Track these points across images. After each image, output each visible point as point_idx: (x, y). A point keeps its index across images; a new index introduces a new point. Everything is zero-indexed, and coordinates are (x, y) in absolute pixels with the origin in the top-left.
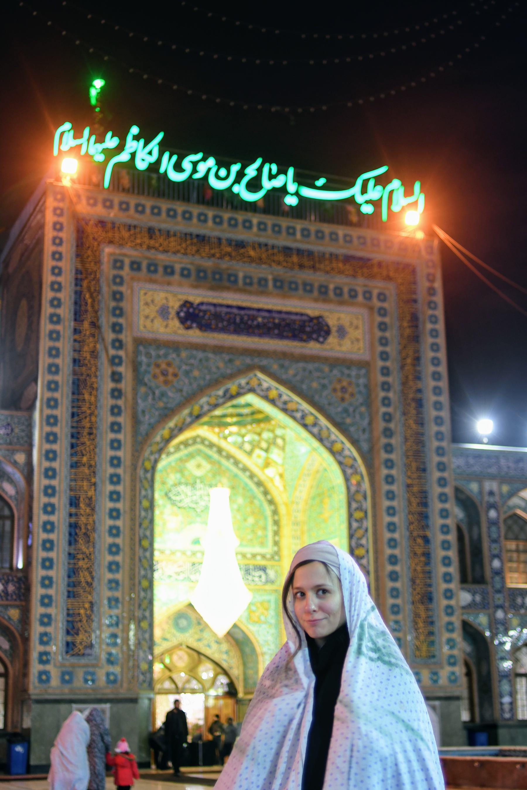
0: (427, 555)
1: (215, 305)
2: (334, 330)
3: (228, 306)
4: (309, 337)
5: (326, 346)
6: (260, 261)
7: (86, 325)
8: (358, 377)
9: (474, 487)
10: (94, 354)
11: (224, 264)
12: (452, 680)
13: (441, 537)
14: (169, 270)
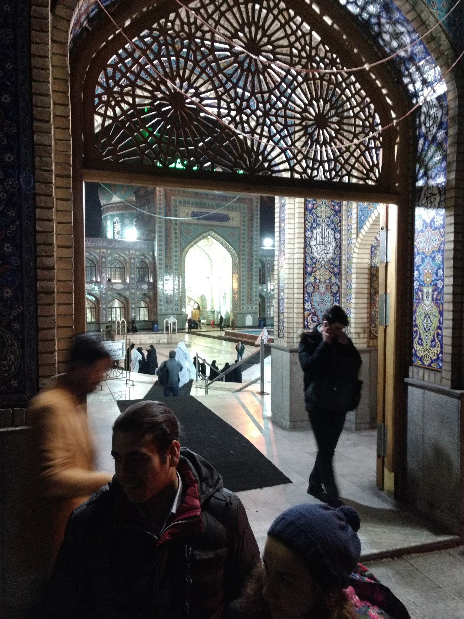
0: (252, 278)
2: (231, 218)
6: (212, 199)
9: (264, 259)
10: (170, 227)
11: (203, 201)
12: (256, 308)
13: (255, 274)
14: (189, 203)
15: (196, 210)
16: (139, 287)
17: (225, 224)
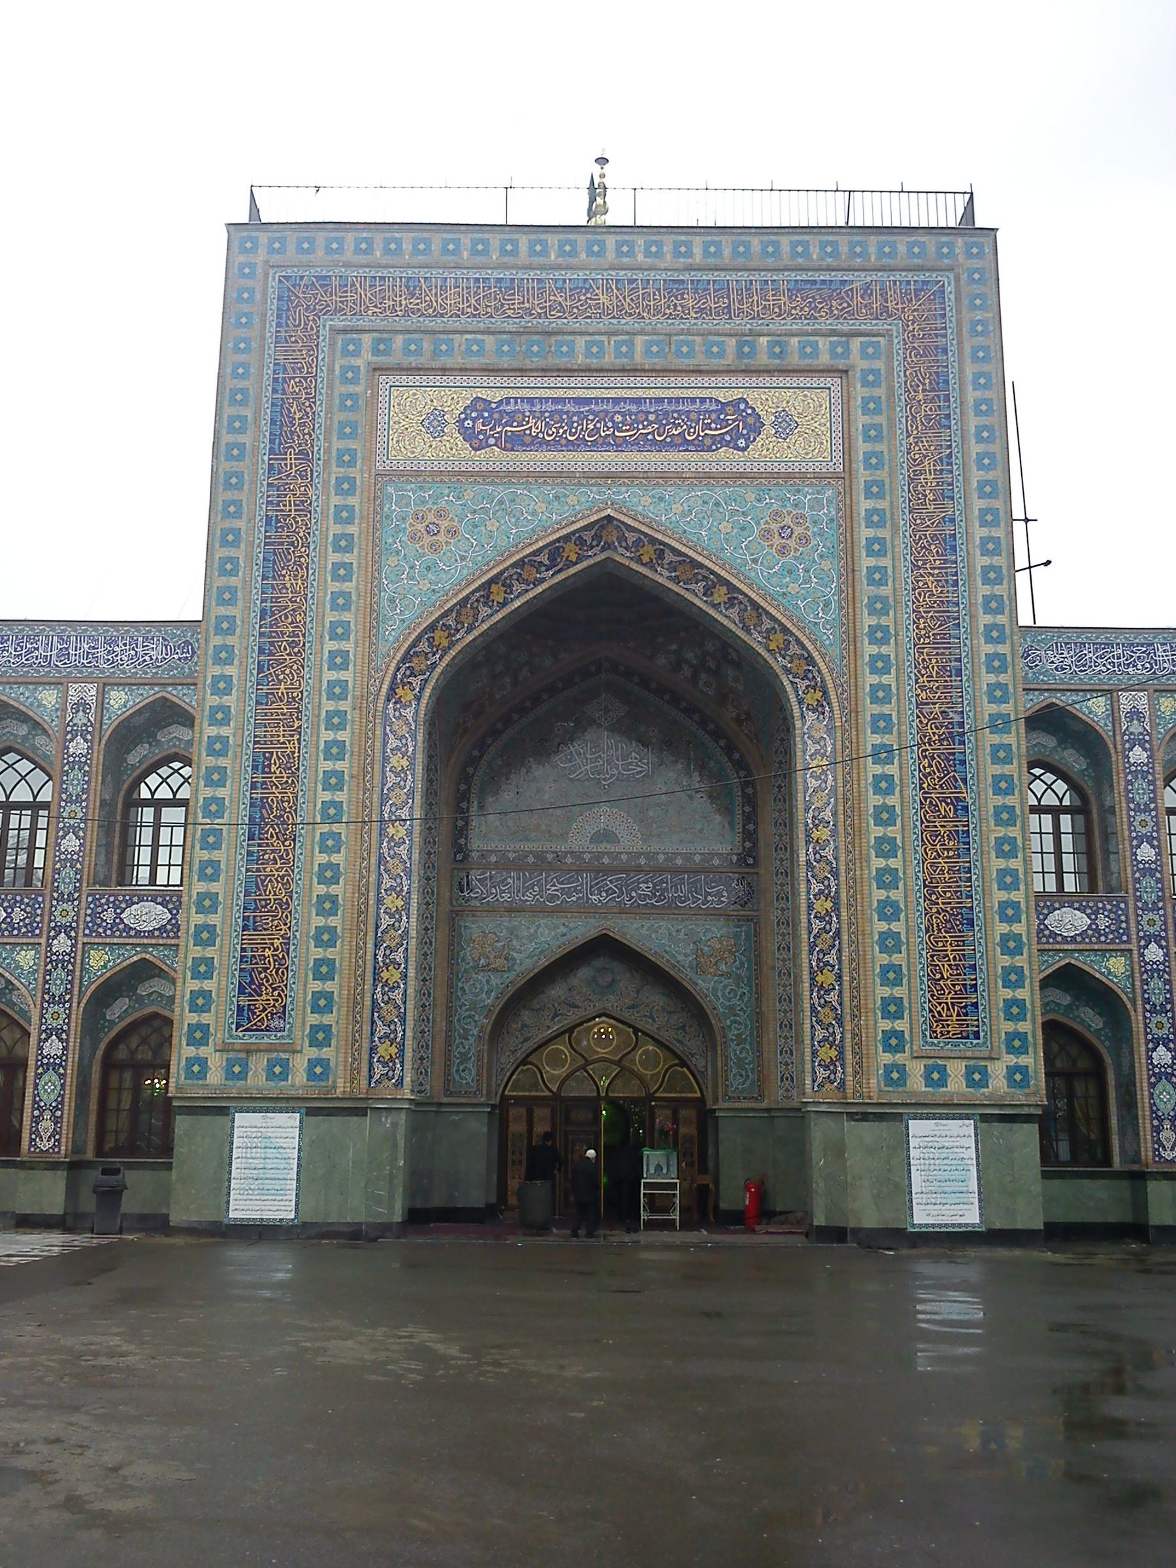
1: (531, 401)
2: (768, 420)
3: (556, 401)
4: (718, 442)
5: (753, 452)
6: (621, 312)
7: (291, 457)
8: (817, 504)
10: (304, 506)
15: (494, 391)
16: (109, 916)
17: (724, 458)
